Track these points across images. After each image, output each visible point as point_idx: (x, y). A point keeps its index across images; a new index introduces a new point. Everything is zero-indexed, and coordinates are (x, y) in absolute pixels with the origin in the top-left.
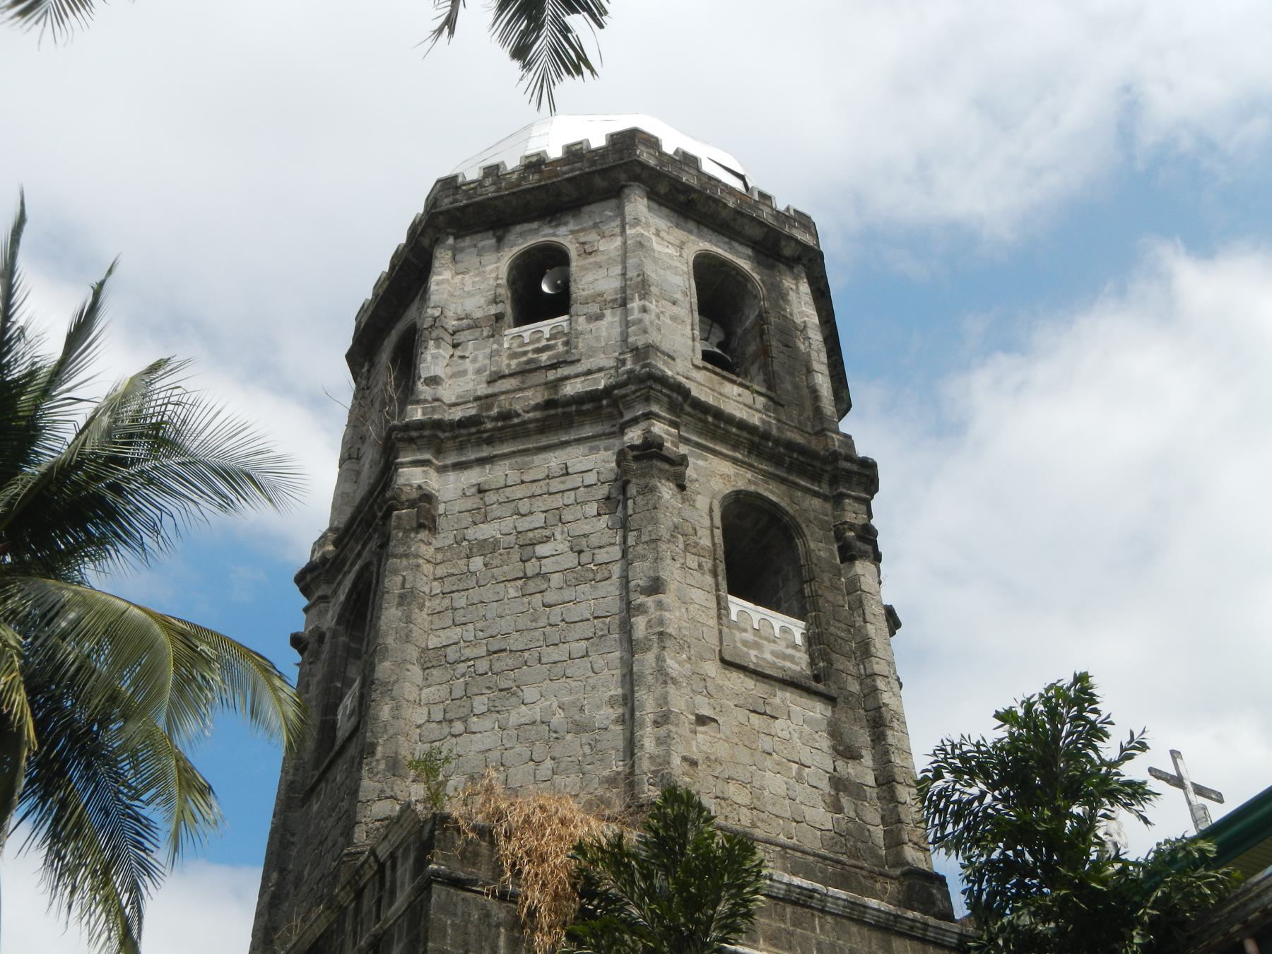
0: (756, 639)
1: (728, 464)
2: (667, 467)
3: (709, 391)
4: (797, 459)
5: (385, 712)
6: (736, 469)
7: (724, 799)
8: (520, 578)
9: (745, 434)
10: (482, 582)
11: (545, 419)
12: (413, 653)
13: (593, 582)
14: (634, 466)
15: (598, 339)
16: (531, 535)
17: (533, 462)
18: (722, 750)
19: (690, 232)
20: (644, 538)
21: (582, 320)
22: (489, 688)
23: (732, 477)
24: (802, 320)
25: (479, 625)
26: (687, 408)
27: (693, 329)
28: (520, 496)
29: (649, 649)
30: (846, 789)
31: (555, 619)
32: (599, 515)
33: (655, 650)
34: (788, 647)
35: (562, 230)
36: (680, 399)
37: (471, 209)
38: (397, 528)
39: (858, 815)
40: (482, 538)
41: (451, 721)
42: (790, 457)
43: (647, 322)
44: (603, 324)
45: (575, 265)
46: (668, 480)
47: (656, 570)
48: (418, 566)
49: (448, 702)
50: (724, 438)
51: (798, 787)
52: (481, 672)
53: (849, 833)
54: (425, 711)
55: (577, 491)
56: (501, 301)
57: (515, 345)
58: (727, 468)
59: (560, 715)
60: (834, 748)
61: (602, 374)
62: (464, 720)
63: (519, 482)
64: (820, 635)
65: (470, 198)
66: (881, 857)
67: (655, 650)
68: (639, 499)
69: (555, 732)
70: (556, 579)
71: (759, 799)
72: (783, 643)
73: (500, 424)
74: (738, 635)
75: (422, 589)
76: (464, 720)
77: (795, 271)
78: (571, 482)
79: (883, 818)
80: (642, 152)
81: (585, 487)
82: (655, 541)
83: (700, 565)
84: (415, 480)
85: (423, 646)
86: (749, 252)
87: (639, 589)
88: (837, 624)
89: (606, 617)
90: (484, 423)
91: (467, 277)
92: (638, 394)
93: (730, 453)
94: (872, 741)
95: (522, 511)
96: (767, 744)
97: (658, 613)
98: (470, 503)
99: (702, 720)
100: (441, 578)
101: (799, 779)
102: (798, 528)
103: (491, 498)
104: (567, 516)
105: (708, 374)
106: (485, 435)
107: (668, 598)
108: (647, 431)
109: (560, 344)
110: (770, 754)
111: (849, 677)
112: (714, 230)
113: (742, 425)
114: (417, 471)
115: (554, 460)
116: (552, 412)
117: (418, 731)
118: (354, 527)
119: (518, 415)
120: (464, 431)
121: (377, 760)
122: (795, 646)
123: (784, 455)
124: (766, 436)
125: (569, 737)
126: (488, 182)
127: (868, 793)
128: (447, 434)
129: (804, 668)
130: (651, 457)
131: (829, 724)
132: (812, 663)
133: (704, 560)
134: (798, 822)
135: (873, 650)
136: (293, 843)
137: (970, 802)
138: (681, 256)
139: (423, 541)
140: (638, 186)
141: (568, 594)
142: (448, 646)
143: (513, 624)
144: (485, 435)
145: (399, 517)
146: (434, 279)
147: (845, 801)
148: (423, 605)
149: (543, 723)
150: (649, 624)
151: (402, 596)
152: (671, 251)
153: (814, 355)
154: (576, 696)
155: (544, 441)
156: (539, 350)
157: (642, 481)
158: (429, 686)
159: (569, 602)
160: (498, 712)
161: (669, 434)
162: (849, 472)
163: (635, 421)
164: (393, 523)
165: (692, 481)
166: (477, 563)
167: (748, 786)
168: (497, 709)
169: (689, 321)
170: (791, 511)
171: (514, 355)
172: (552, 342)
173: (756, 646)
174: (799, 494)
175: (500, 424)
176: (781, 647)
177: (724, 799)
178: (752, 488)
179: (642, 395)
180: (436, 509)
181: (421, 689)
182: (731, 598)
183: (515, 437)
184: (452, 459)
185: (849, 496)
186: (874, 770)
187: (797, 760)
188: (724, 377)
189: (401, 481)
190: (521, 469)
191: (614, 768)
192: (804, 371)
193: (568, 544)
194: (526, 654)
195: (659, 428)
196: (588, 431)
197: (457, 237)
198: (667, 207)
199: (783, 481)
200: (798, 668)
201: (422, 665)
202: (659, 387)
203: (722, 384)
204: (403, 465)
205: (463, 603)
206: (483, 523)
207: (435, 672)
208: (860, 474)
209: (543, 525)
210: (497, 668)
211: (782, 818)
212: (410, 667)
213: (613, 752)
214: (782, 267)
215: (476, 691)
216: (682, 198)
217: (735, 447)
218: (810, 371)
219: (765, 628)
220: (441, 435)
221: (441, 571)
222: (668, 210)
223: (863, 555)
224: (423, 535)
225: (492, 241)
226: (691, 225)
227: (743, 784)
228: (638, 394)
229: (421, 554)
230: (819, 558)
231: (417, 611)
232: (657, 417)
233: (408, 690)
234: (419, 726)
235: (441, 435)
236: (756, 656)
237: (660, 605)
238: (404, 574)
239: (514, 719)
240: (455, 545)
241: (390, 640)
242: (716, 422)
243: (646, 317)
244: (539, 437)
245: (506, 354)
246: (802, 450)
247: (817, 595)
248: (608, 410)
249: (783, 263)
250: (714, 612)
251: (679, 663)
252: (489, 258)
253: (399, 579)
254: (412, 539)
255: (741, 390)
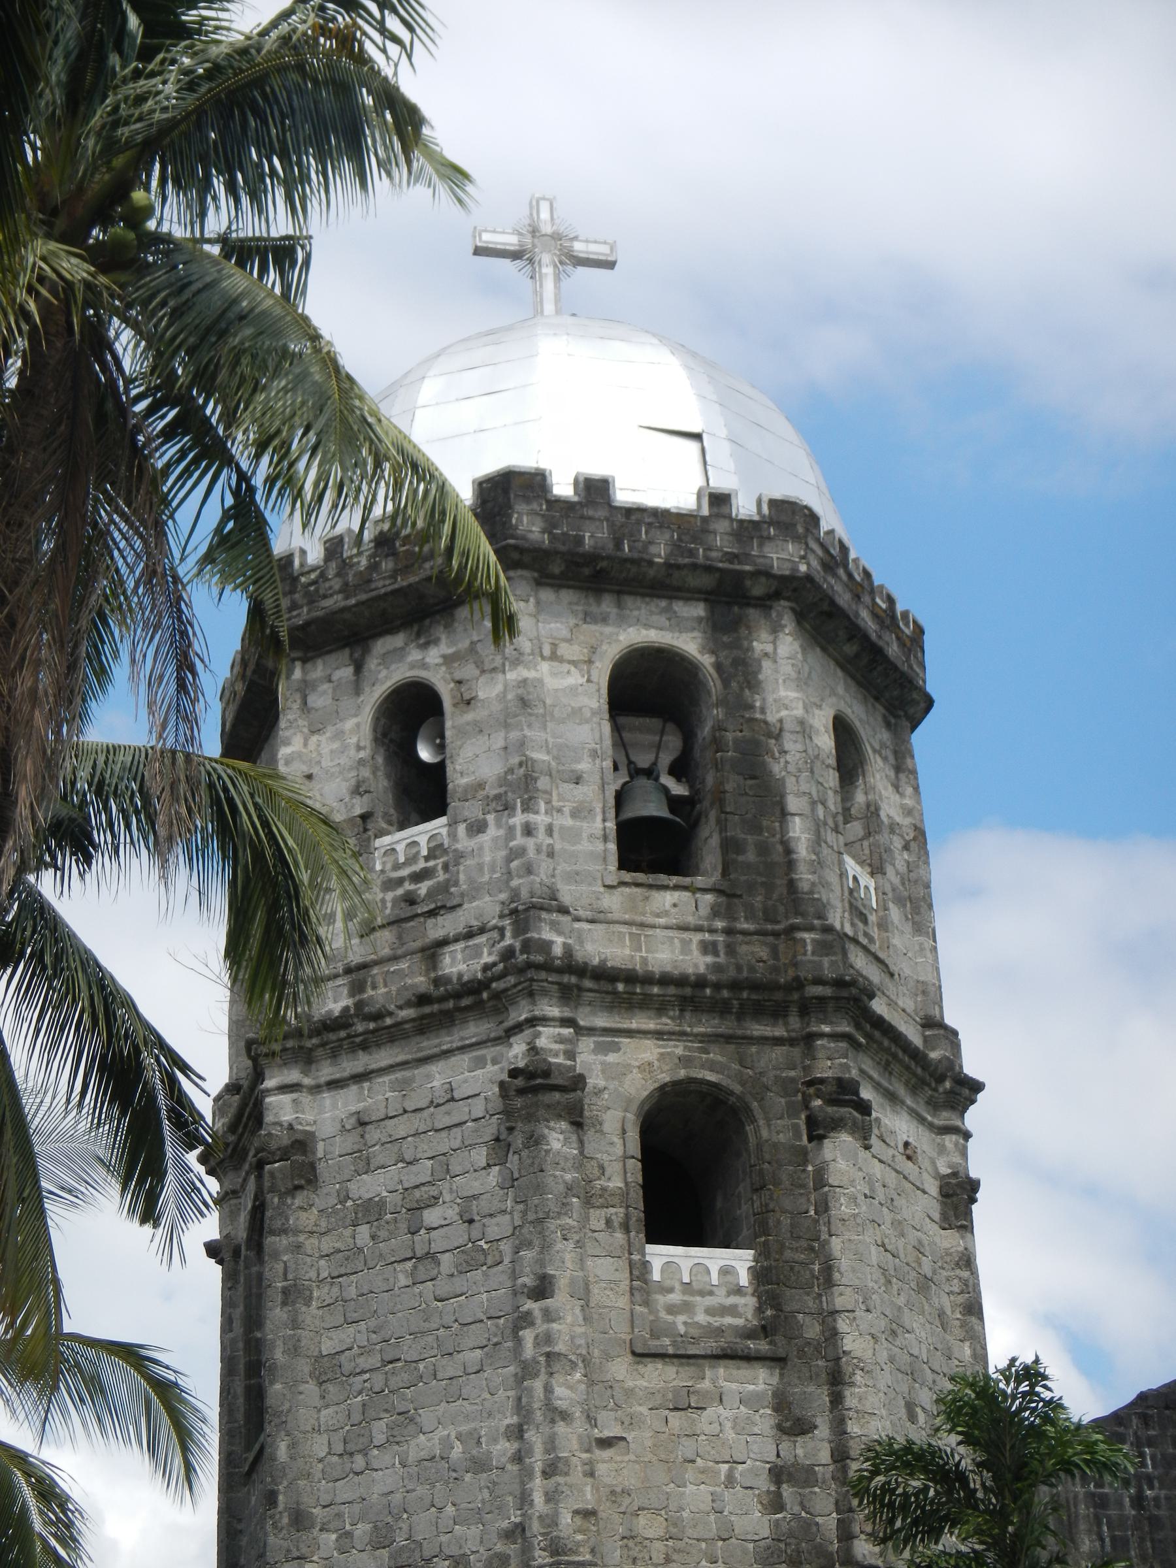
0: (686, 1298)
1: (649, 1043)
2: (557, 1096)
3: (623, 929)
4: (748, 999)
5: (282, 1450)
6: (659, 1047)
7: (633, 1537)
8: (411, 1258)
9: (672, 990)
10: (371, 1264)
11: (422, 1017)
12: (304, 1366)
13: (484, 1268)
14: (519, 1102)
15: (480, 867)
16: (417, 1194)
17: (411, 1080)
18: (629, 1478)
19: (604, 620)
20: (531, 1216)
21: (461, 829)
22: (386, 1411)
23: (656, 1063)
24: (778, 716)
25: (372, 1323)
26: (588, 983)
27: (604, 820)
28: (403, 1134)
29: (537, 1375)
30: (792, 1479)
31: (448, 1319)
32: (489, 1165)
33: (543, 1377)
34: (729, 1294)
35: (433, 655)
36: (573, 980)
37: (313, 627)
38: (272, 1190)
39: (804, 1508)
40: (367, 1196)
41: (351, 1454)
42: (738, 999)
43: (531, 853)
44: (486, 838)
45: (453, 720)
46: (559, 1117)
47: (541, 1263)
48: (298, 1247)
49: (347, 1428)
50: (644, 1004)
51: (727, 1495)
52: (377, 1389)
53: (791, 1534)
54: (324, 1439)
55: (464, 1127)
56: (366, 792)
57: (389, 866)
58: (648, 1051)
59: (458, 1449)
60: (780, 1427)
61: (481, 939)
62: (364, 1452)
63: (401, 1111)
64: (768, 1269)
65: (312, 599)
66: (831, 1554)
67: (543, 1377)
68: (525, 1153)
69: (454, 1471)
70: (446, 1259)
71: (675, 1525)
72: (722, 1292)
73: (372, 1026)
74: (661, 1300)
75: (307, 1277)
76: (364, 1452)
77: (774, 615)
78: (459, 1112)
79: (837, 1503)
80: (519, 520)
81: (474, 1120)
82: (540, 1221)
83: (608, 1222)
84: (285, 1115)
85: (315, 1354)
86: (698, 610)
87: (526, 1290)
88: (795, 1244)
89: (499, 1317)
90: (351, 1025)
91: (323, 738)
92: (520, 988)
93: (651, 1025)
94: (831, 1402)
95: (408, 1158)
96: (687, 1448)
97: (545, 1326)
98: (350, 1142)
99: (606, 1443)
100: (327, 1256)
101: (730, 1481)
102: (748, 1109)
103: (374, 1134)
104: (455, 1168)
105: (627, 890)
106: (358, 1040)
107: (560, 1300)
108: (533, 1050)
109: (440, 867)
110: (693, 1461)
111: (808, 1319)
112: (643, 595)
113: (665, 980)
114: (286, 1098)
115: (437, 1077)
116: (427, 1010)
117: (320, 1466)
118: (245, 1119)
119: (391, 1014)
120: (332, 1036)
121: (280, 1513)
122: (738, 1291)
123: (730, 999)
124: (700, 983)
125: (468, 1477)
126: (331, 573)
127: (820, 1476)
128: (315, 1041)
129: (750, 1317)
130: (535, 1090)
131: (775, 1394)
132: (759, 1310)
133: (612, 1210)
134: (724, 1540)
135: (836, 1276)
136: (241, 1531)
137: (916, 1495)
138: (589, 681)
139: (301, 1208)
140: (521, 577)
141: (460, 1284)
142: (342, 1352)
143: (405, 1324)
144: (358, 1040)
145: (272, 1174)
146: (284, 752)
147: (787, 1491)
148: (311, 1298)
149: (443, 1458)
150: (537, 1344)
151: (285, 1292)
152: (575, 678)
153: (790, 784)
154: (473, 1425)
155: (429, 1044)
156: (418, 877)
157: (527, 1128)
158: (327, 1406)
159: (461, 1295)
160: (397, 1443)
161: (561, 1040)
162: (821, 999)
163: (518, 1028)
164: (267, 1184)
165: (599, 1092)
166: (364, 1231)
167: (663, 1512)
168: (397, 1439)
169: (598, 810)
170: (737, 1088)
171: (391, 884)
172: (431, 863)
173: (687, 1308)
174: (754, 1049)
175: (372, 1026)
176: (721, 1298)
177: (633, 1537)
178: (682, 1073)
179: (523, 989)
180: (314, 1153)
181: (319, 1411)
182: (651, 1248)
183: (392, 1040)
184: (327, 1072)
185: (822, 1035)
186: (830, 1442)
187: (727, 1458)
188: (650, 887)
189: (269, 1118)
190: (403, 1087)
191: (513, 1519)
192: (778, 813)
193: (457, 1209)
194: (421, 1366)
195: (547, 1037)
196: (474, 1030)
197: (305, 661)
198: (569, 587)
199: (728, 1039)
200: (739, 1322)
201: (318, 1379)
202: (543, 975)
203: (647, 898)
204: (268, 1091)
205: (352, 1292)
206: (366, 1173)
207: (330, 1387)
208: (837, 999)
209: (429, 1179)
210: (394, 1382)
211: (704, 1540)
212: (302, 1388)
213: (510, 1498)
214: (753, 613)
215: (374, 1414)
216: (587, 571)
217: (661, 1008)
218: (784, 814)
219: (699, 1277)
220: (309, 1043)
221: (327, 1244)
222: (571, 592)
223: (836, 1125)
224: (299, 1200)
225: (346, 672)
226: (607, 605)
227: (656, 1511)
228: (520, 988)
229: (301, 1228)
230: (775, 1145)
231: (304, 1309)
232: (544, 1020)
233: (305, 1417)
234: (321, 1461)
235: (309, 1043)
236: (685, 1323)
237: (548, 1316)
238: (285, 1258)
239: (412, 1457)
240: (339, 1206)
241: (279, 1355)
242: (630, 989)
243: (530, 843)
244: (418, 1039)
245: (379, 882)
246: (755, 986)
247: (768, 1212)
248: (490, 1004)
249: (755, 606)
250: (625, 1285)
251: (570, 1388)
252: (347, 703)
253: (280, 1267)
254: (289, 1207)
255: (677, 894)
